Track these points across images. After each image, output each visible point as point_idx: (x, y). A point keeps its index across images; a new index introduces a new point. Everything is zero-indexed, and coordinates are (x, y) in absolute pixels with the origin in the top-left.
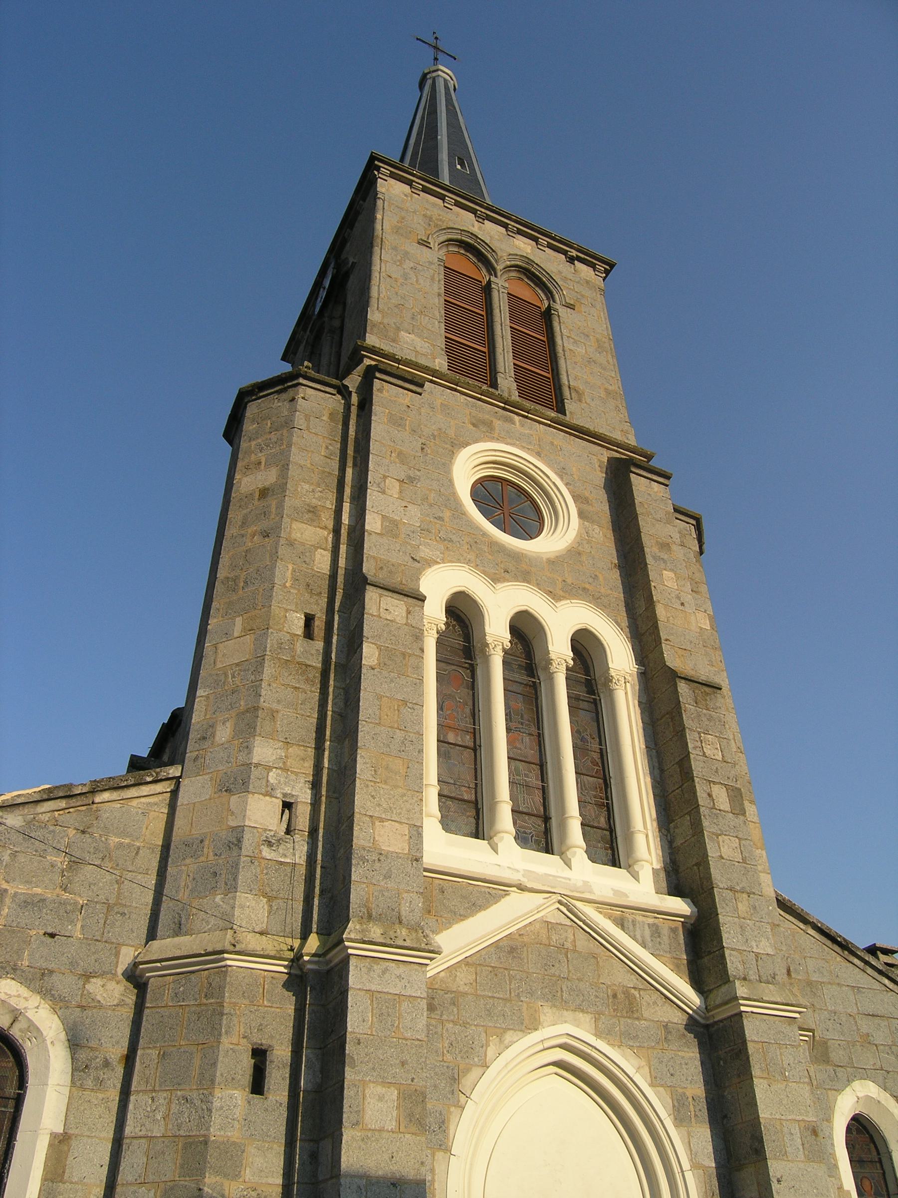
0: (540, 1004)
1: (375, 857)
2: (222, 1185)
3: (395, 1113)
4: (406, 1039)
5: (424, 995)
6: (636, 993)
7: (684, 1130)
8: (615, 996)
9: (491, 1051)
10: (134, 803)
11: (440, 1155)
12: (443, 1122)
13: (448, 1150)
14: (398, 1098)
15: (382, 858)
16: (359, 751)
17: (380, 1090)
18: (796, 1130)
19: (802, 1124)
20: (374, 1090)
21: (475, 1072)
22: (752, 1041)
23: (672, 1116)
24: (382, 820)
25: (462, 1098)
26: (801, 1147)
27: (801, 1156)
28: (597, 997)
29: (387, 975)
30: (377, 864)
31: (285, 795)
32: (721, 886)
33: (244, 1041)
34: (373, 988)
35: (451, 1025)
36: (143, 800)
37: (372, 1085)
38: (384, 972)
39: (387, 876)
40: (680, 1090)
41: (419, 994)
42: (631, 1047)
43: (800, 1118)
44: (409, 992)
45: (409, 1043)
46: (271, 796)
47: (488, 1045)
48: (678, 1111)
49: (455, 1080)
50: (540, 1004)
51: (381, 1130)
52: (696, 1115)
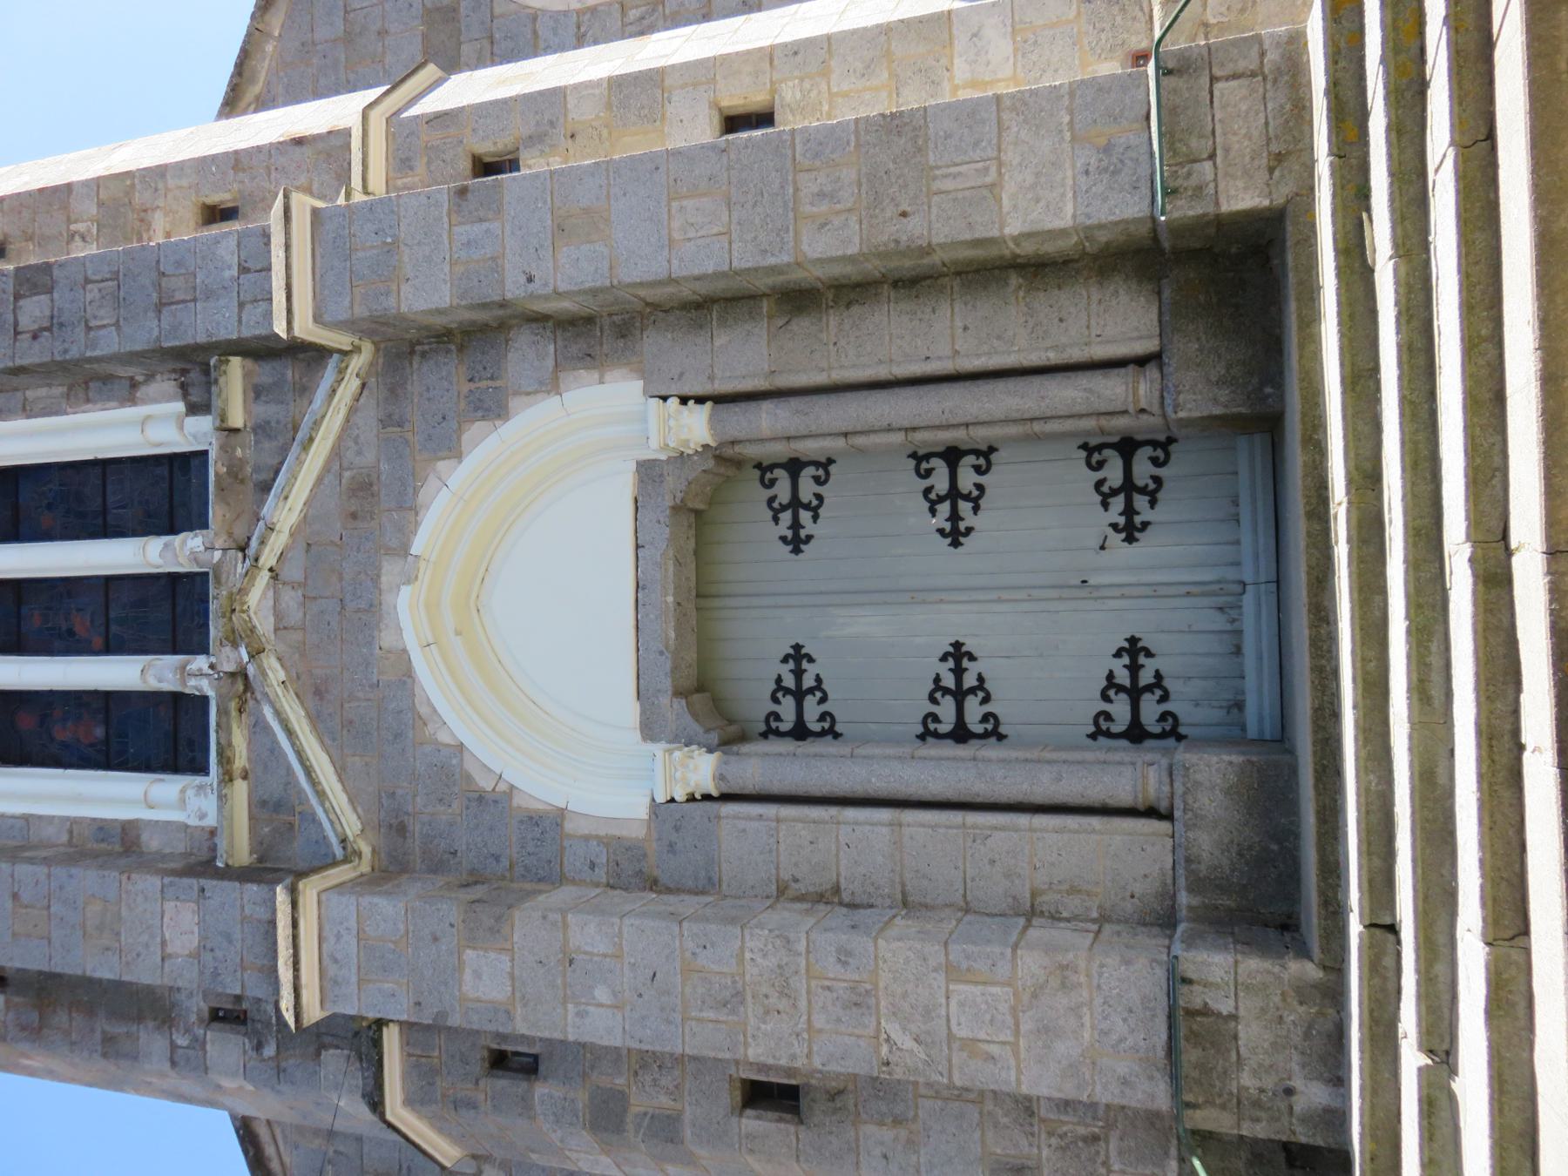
0: (377, 650)
1: (207, 957)
2: (637, 1115)
3: (492, 955)
4: (407, 932)
5: (353, 899)
6: (347, 474)
7: (514, 403)
8: (354, 516)
9: (443, 737)
10: (287, 1160)
11: (569, 826)
12: (531, 818)
13: (562, 813)
14: (475, 949)
15: (209, 946)
16: (88, 973)
17: (468, 975)
18: (464, 231)
19: (454, 216)
20: (470, 986)
21: (469, 766)
22: (352, 307)
23: (497, 423)
24: (164, 943)
25: (502, 787)
26: (485, 225)
27: (495, 226)
28: (359, 550)
29: (339, 957)
30: (219, 954)
31: (201, 1020)
32: (156, 333)
33: (482, 1083)
34: (354, 979)
35: (418, 799)
36: (282, 1148)
37: (464, 988)
38: (336, 961)
39: (229, 938)
40: (463, 404)
41: (353, 908)
42: (416, 492)
43: (446, 219)
44: (353, 923)
45: (411, 928)
46: (204, 1043)
47: (436, 742)
48: (488, 410)
49: (481, 799)
50: (377, 650)
51: (512, 976)
52: (492, 378)
